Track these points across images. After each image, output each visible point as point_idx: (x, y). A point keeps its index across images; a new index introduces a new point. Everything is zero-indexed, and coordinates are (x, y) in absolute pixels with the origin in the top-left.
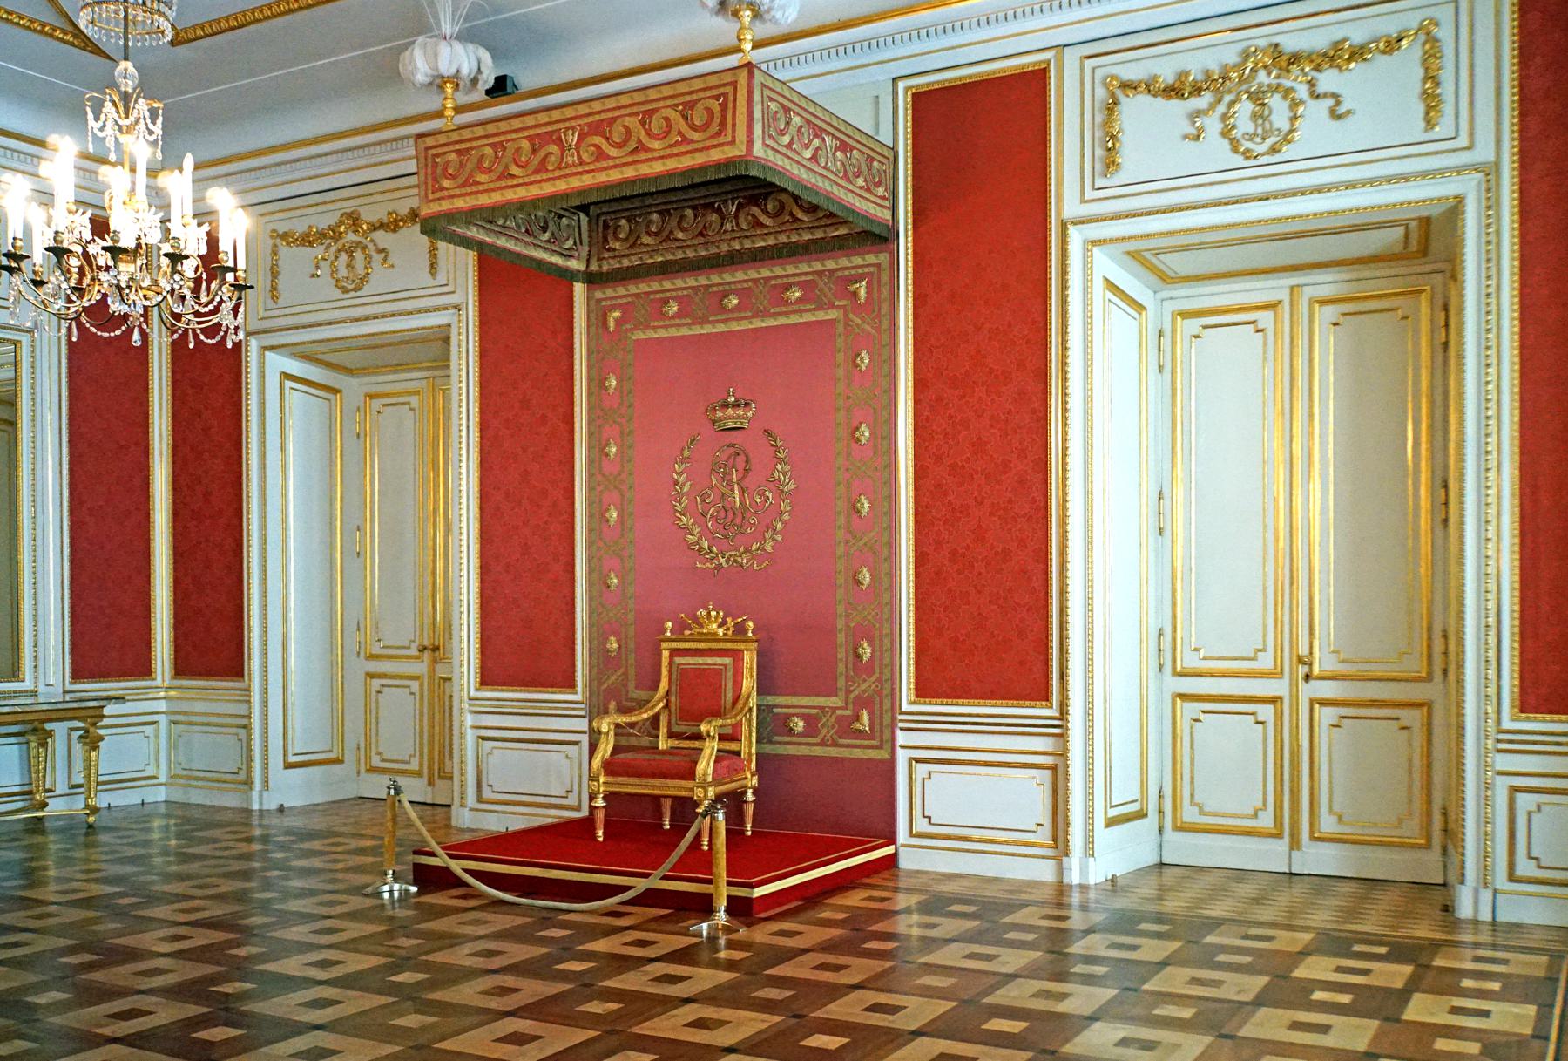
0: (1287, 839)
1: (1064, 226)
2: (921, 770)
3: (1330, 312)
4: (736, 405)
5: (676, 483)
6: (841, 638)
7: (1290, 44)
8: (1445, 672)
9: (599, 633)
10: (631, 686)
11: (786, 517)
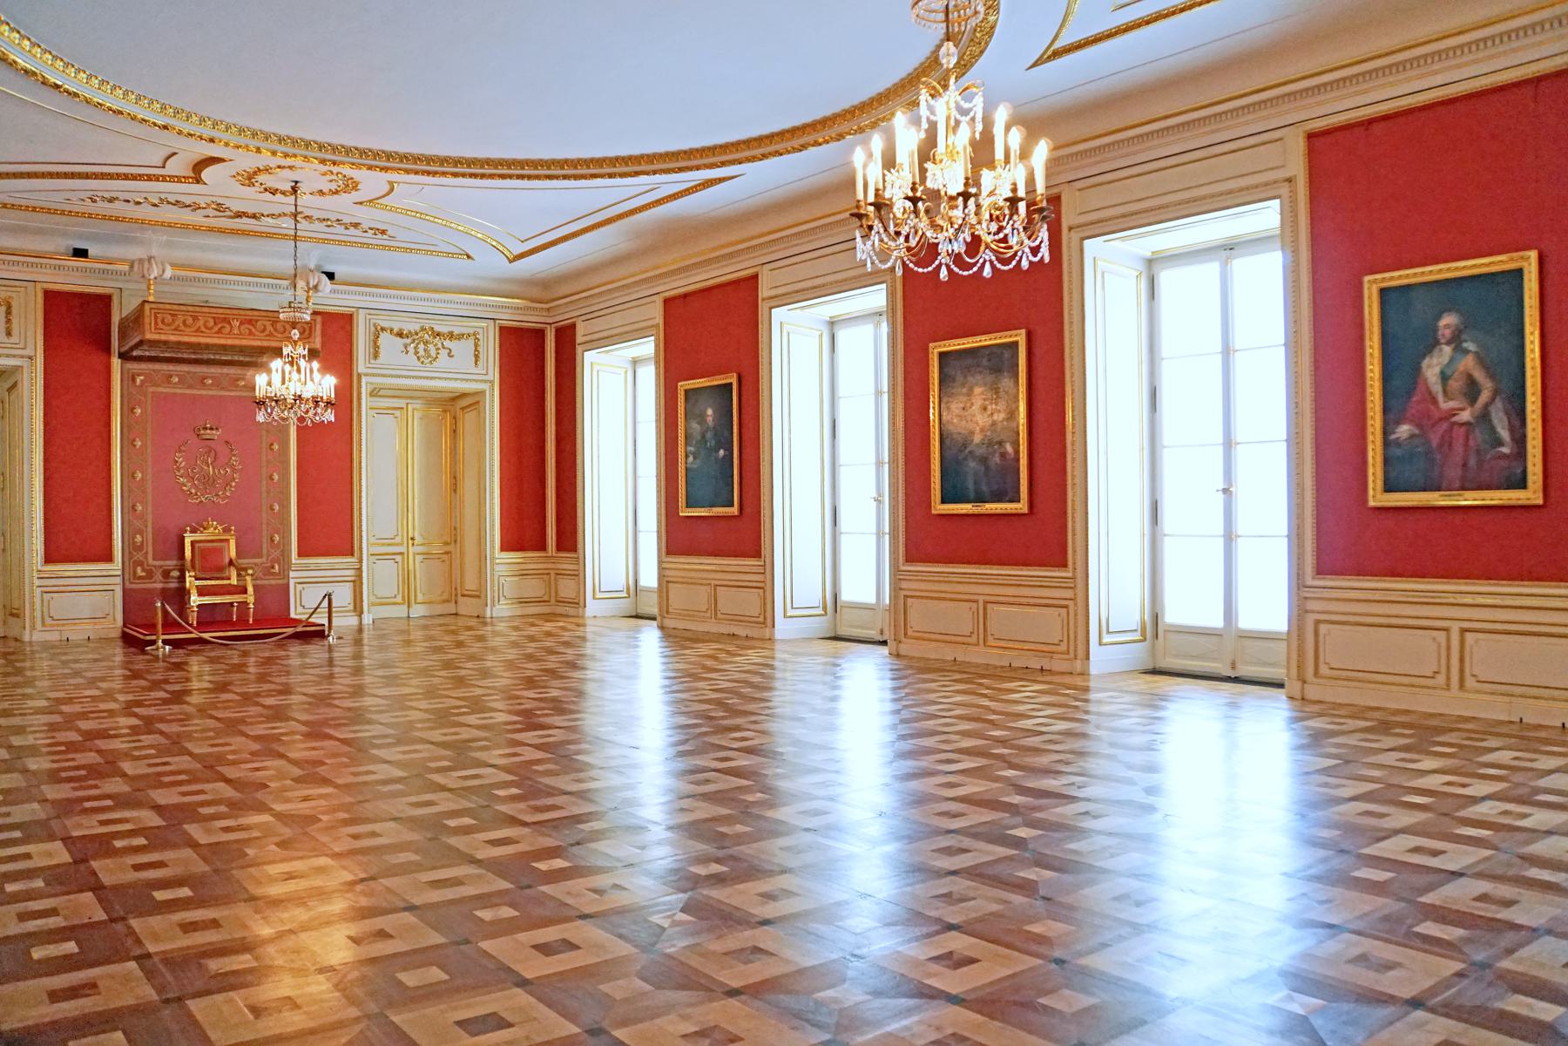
1: (359, 376)
7: (437, 329)
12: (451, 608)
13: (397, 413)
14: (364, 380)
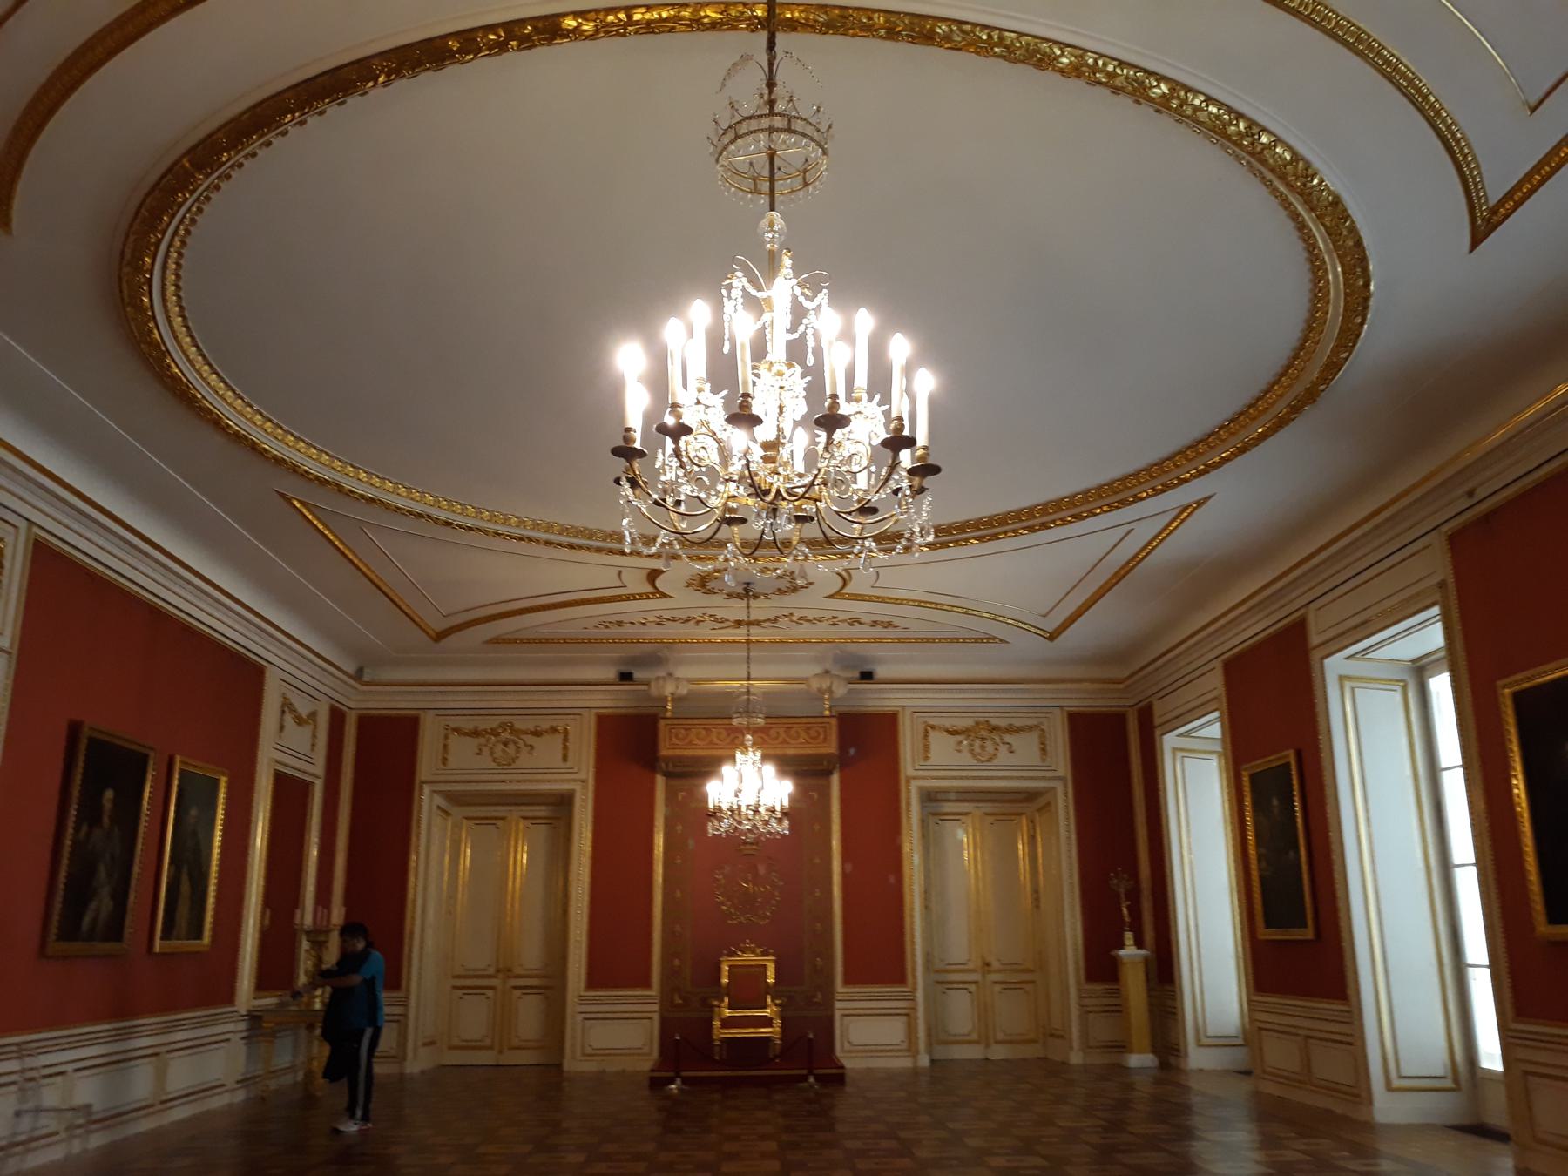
3: (991, 819)
14: (914, 785)
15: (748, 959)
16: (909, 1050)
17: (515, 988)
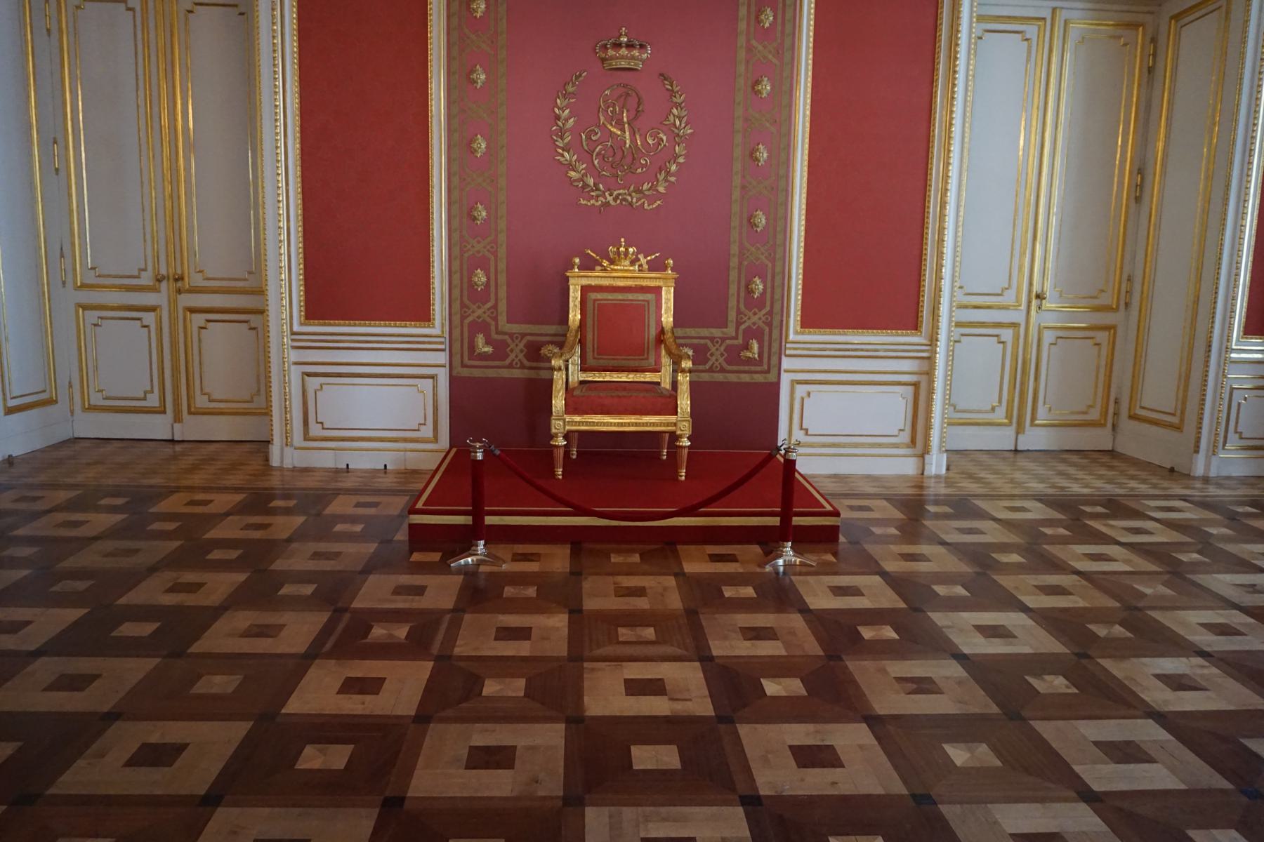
0: (1014, 425)
2: (801, 390)
4: (630, 46)
5: (558, 118)
6: (733, 275)
8: (1127, 305)
9: (462, 265)
10: (502, 319)
11: (681, 160)
12: (1099, 439)
13: (1031, 31)
15: (625, 273)
16: (913, 441)
17: (193, 310)
